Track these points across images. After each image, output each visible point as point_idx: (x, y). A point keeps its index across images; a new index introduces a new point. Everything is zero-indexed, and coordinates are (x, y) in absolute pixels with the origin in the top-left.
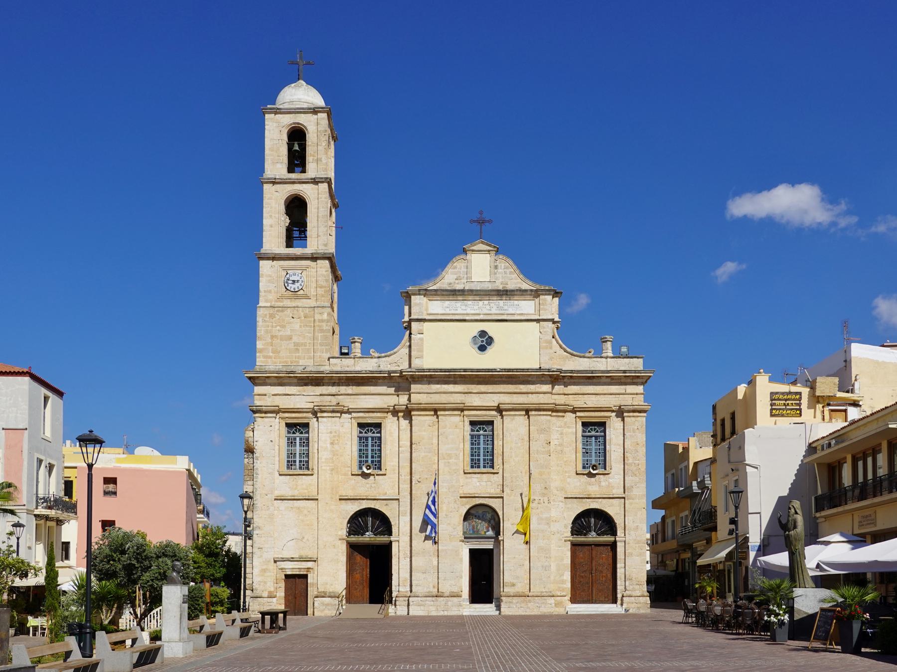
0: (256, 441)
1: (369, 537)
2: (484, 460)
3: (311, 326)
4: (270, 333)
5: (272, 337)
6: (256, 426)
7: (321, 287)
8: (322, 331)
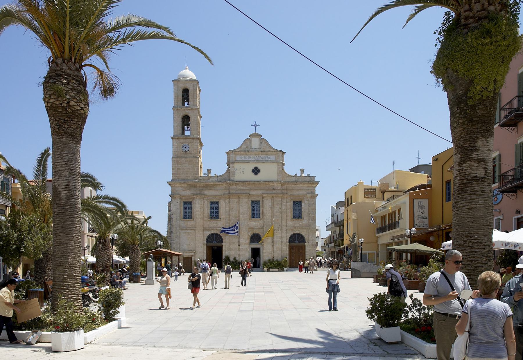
1: (215, 244)
2: (257, 215)
5: (178, 169)
7: (196, 150)
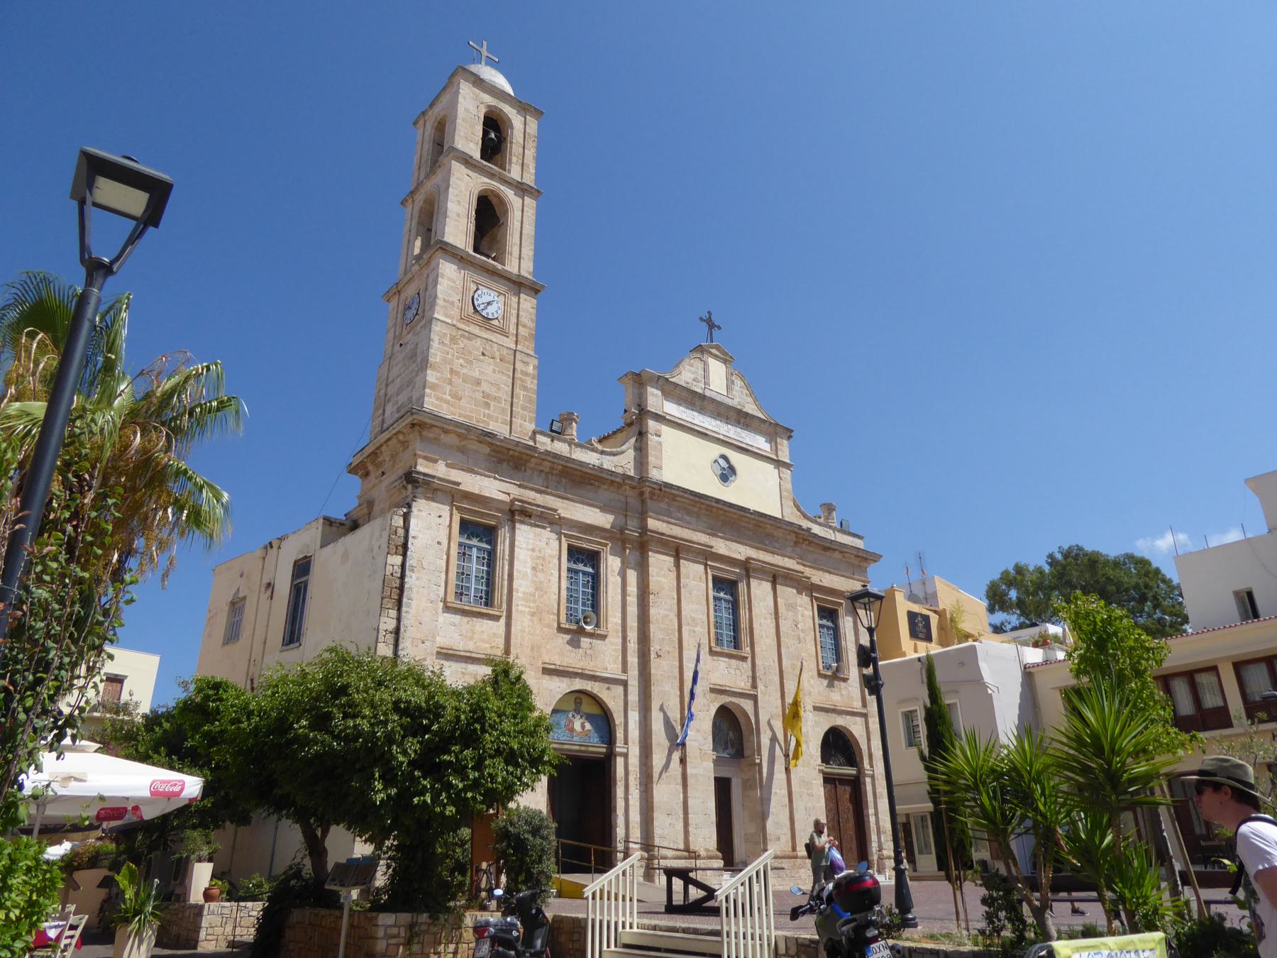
0: (413, 537)
3: (509, 376)
5: (452, 371)
6: (414, 509)
7: (524, 326)
8: (525, 388)
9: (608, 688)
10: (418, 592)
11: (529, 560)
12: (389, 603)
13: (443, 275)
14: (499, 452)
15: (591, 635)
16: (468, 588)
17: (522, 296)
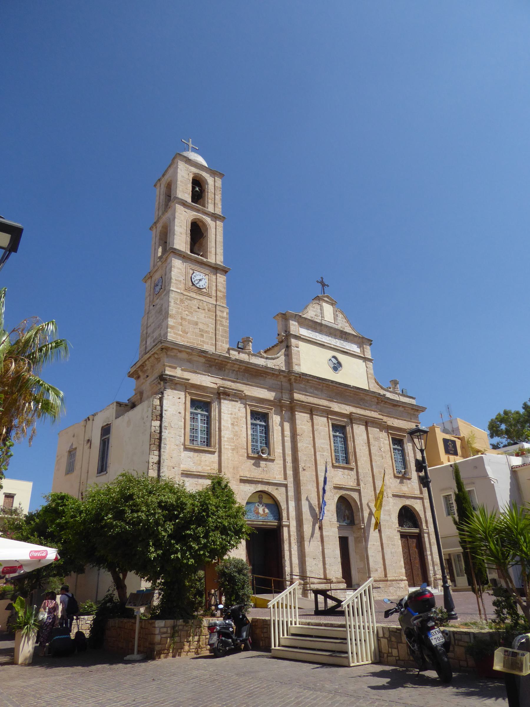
0: (165, 410)
3: (213, 319)
4: (180, 314)
5: (182, 318)
7: (220, 291)
8: (222, 325)
9: (277, 489)
10: (169, 440)
11: (229, 420)
12: (154, 447)
13: (174, 266)
14: (210, 361)
15: (266, 460)
16: (197, 437)
17: (218, 274)
